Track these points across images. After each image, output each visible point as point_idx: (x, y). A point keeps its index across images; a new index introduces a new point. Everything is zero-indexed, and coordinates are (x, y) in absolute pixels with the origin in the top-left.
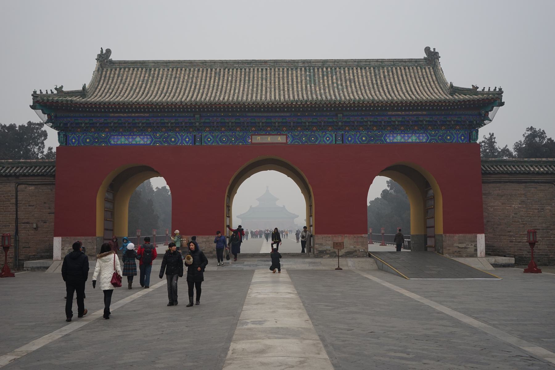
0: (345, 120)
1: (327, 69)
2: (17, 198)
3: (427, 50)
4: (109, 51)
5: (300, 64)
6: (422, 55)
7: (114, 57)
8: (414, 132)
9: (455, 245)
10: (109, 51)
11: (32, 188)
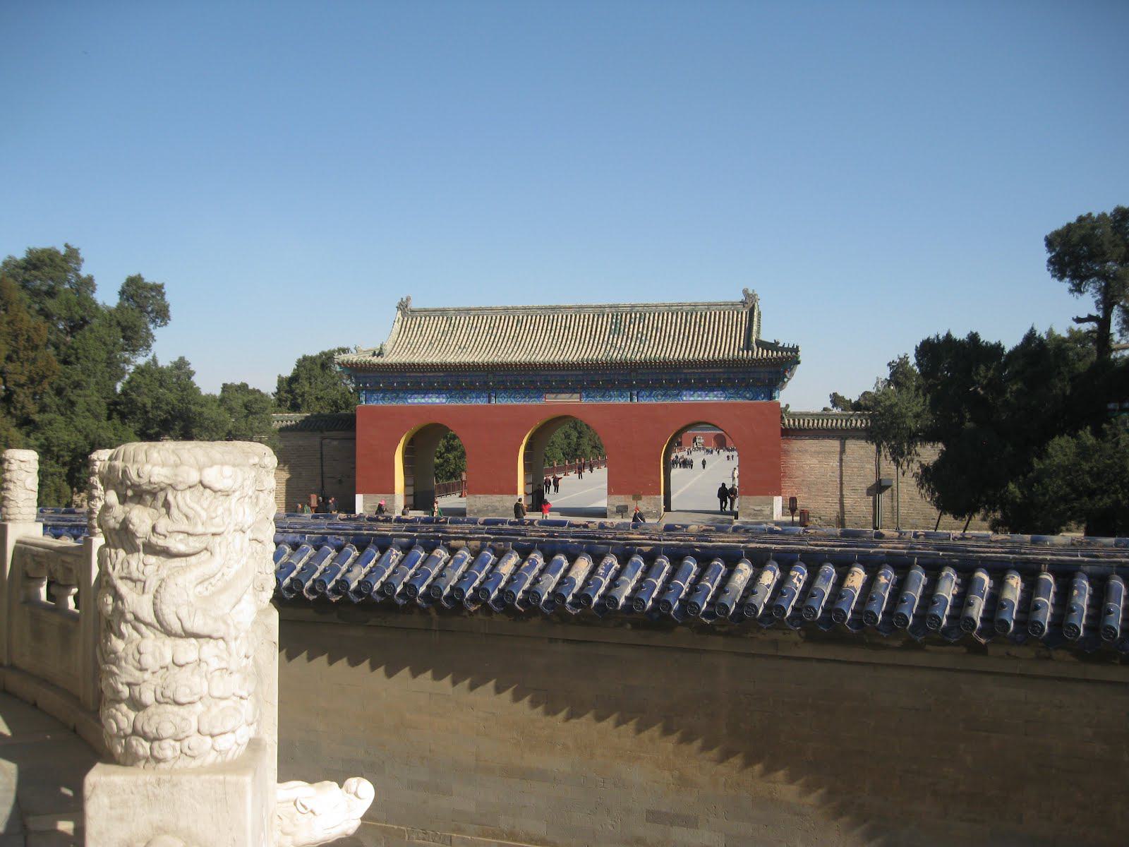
0: (640, 377)
1: (636, 315)
2: (322, 453)
3: (745, 292)
4: (408, 299)
5: (607, 310)
6: (741, 297)
7: (414, 305)
8: (712, 390)
9: (751, 507)
10: (408, 299)
11: (335, 443)
